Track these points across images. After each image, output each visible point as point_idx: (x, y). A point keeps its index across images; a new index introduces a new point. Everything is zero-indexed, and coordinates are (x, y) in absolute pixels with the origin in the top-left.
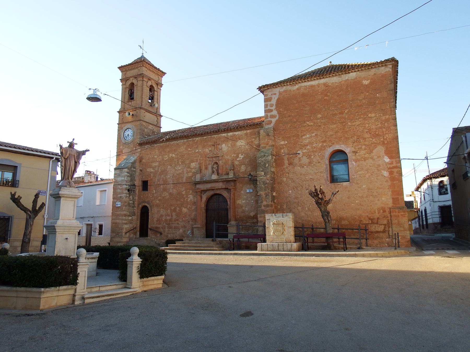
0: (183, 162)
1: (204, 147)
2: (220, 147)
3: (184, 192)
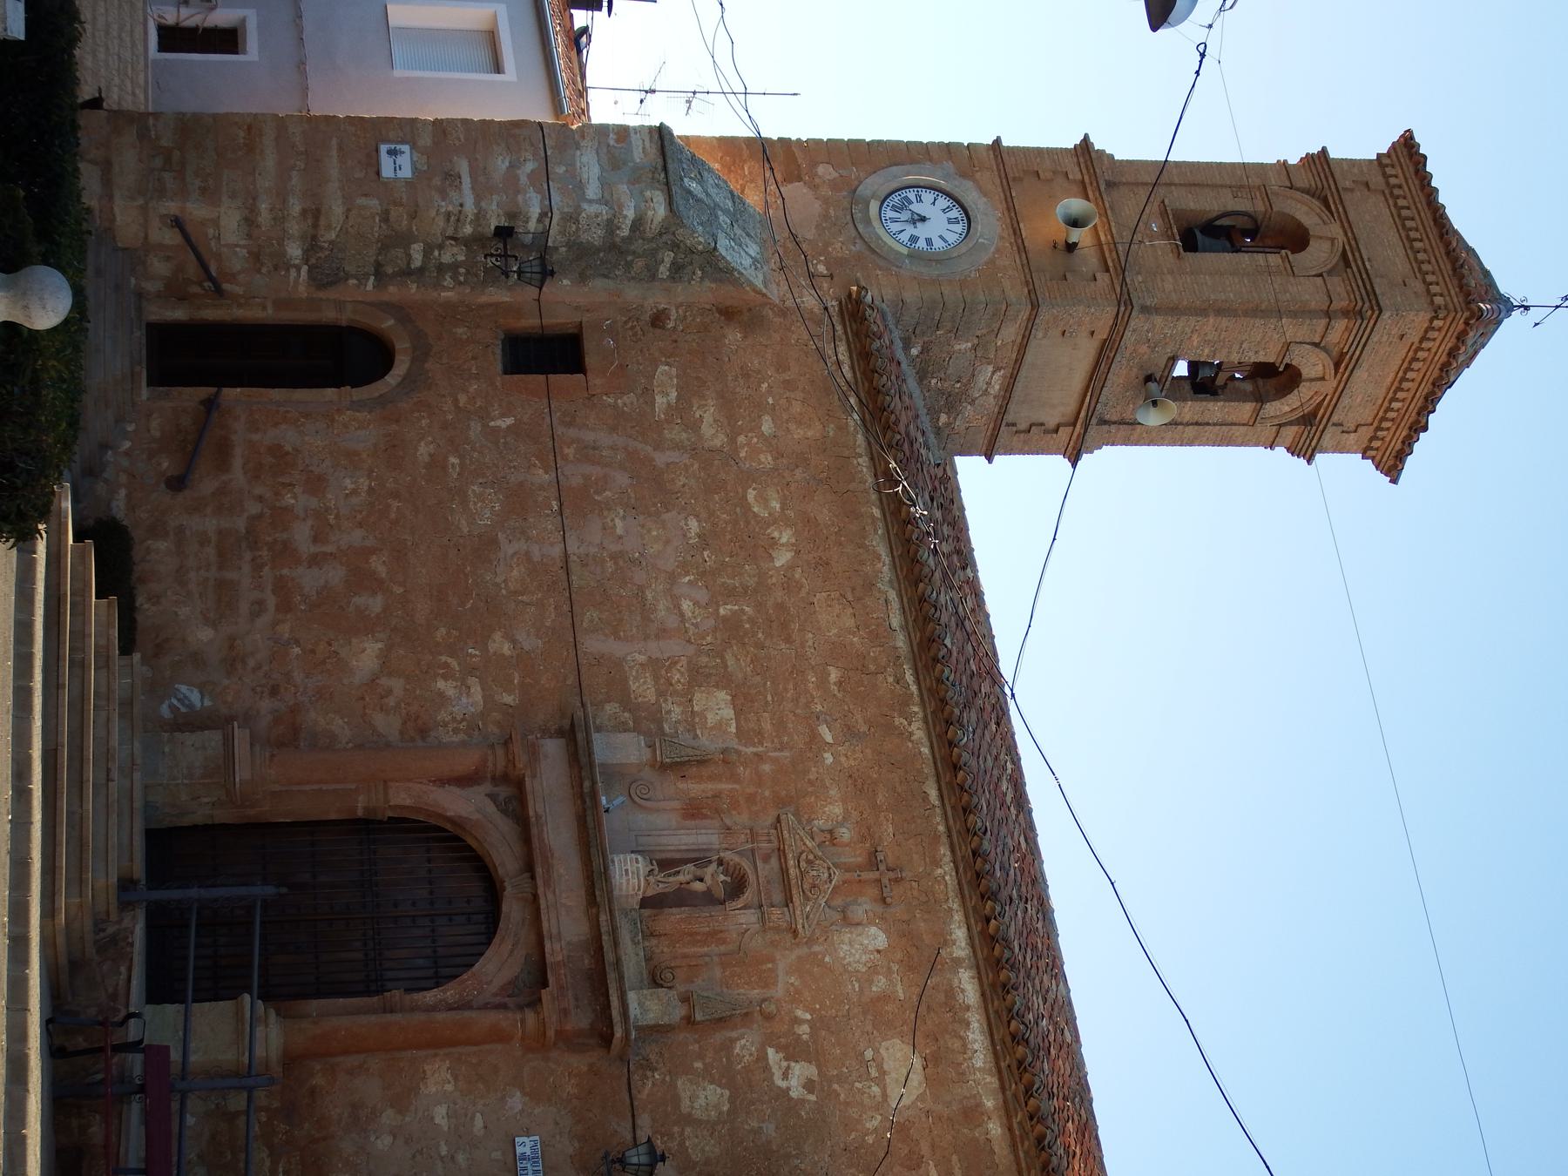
0: (731, 629)
1: (859, 786)
2: (863, 907)
3: (506, 649)
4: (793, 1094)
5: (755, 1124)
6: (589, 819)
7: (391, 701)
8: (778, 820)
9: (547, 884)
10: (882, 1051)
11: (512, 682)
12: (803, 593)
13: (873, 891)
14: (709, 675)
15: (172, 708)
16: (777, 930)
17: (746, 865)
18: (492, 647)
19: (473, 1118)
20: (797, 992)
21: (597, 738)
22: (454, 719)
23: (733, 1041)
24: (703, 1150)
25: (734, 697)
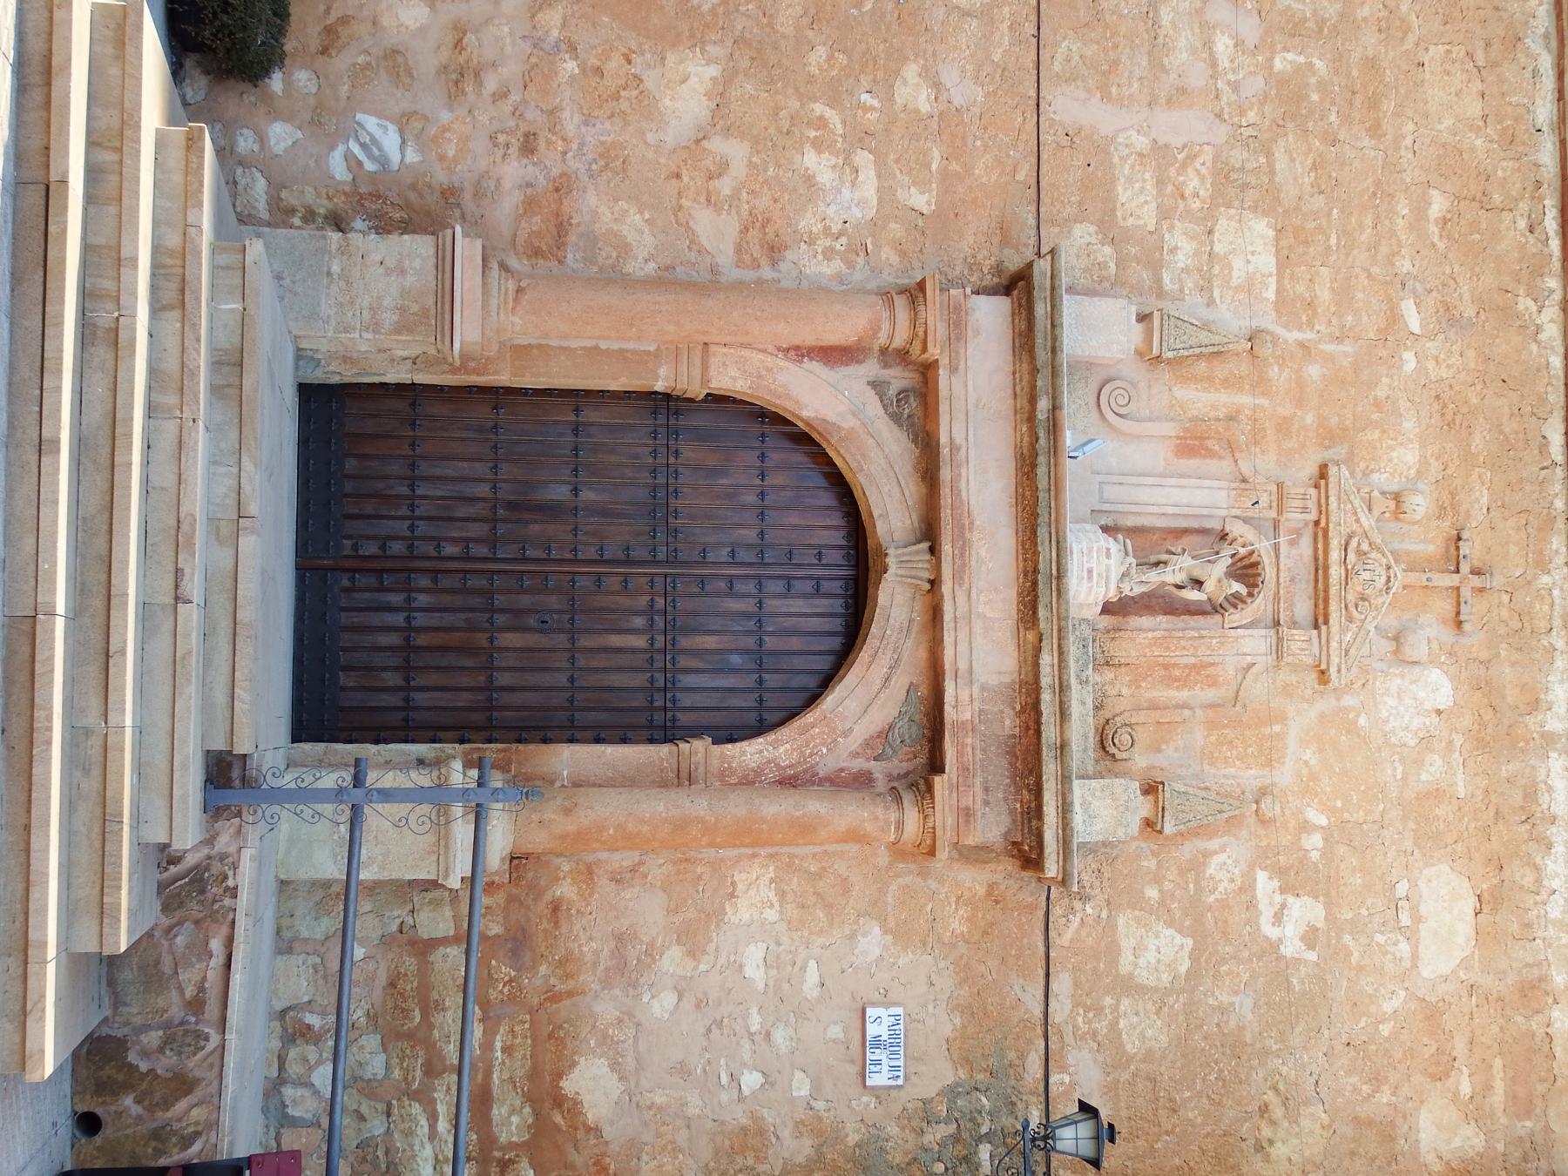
0: (1289, 95)
1: (1451, 417)
2: (1430, 631)
3: (923, 101)
4: (1288, 950)
5: (1225, 998)
6: (1041, 471)
7: (725, 186)
8: (1323, 473)
9: (958, 577)
10: (1422, 885)
11: (928, 166)
12: (1411, 39)
13: (1445, 606)
14: (1245, 187)
15: (352, 163)
16: (1296, 668)
17: (1263, 547)
18: (902, 94)
19: (803, 969)
20: (1314, 777)
21: (1070, 306)
22: (827, 229)
23: (1207, 855)
24: (1143, 1036)
25: (1279, 231)
